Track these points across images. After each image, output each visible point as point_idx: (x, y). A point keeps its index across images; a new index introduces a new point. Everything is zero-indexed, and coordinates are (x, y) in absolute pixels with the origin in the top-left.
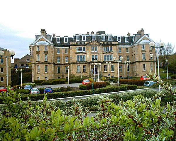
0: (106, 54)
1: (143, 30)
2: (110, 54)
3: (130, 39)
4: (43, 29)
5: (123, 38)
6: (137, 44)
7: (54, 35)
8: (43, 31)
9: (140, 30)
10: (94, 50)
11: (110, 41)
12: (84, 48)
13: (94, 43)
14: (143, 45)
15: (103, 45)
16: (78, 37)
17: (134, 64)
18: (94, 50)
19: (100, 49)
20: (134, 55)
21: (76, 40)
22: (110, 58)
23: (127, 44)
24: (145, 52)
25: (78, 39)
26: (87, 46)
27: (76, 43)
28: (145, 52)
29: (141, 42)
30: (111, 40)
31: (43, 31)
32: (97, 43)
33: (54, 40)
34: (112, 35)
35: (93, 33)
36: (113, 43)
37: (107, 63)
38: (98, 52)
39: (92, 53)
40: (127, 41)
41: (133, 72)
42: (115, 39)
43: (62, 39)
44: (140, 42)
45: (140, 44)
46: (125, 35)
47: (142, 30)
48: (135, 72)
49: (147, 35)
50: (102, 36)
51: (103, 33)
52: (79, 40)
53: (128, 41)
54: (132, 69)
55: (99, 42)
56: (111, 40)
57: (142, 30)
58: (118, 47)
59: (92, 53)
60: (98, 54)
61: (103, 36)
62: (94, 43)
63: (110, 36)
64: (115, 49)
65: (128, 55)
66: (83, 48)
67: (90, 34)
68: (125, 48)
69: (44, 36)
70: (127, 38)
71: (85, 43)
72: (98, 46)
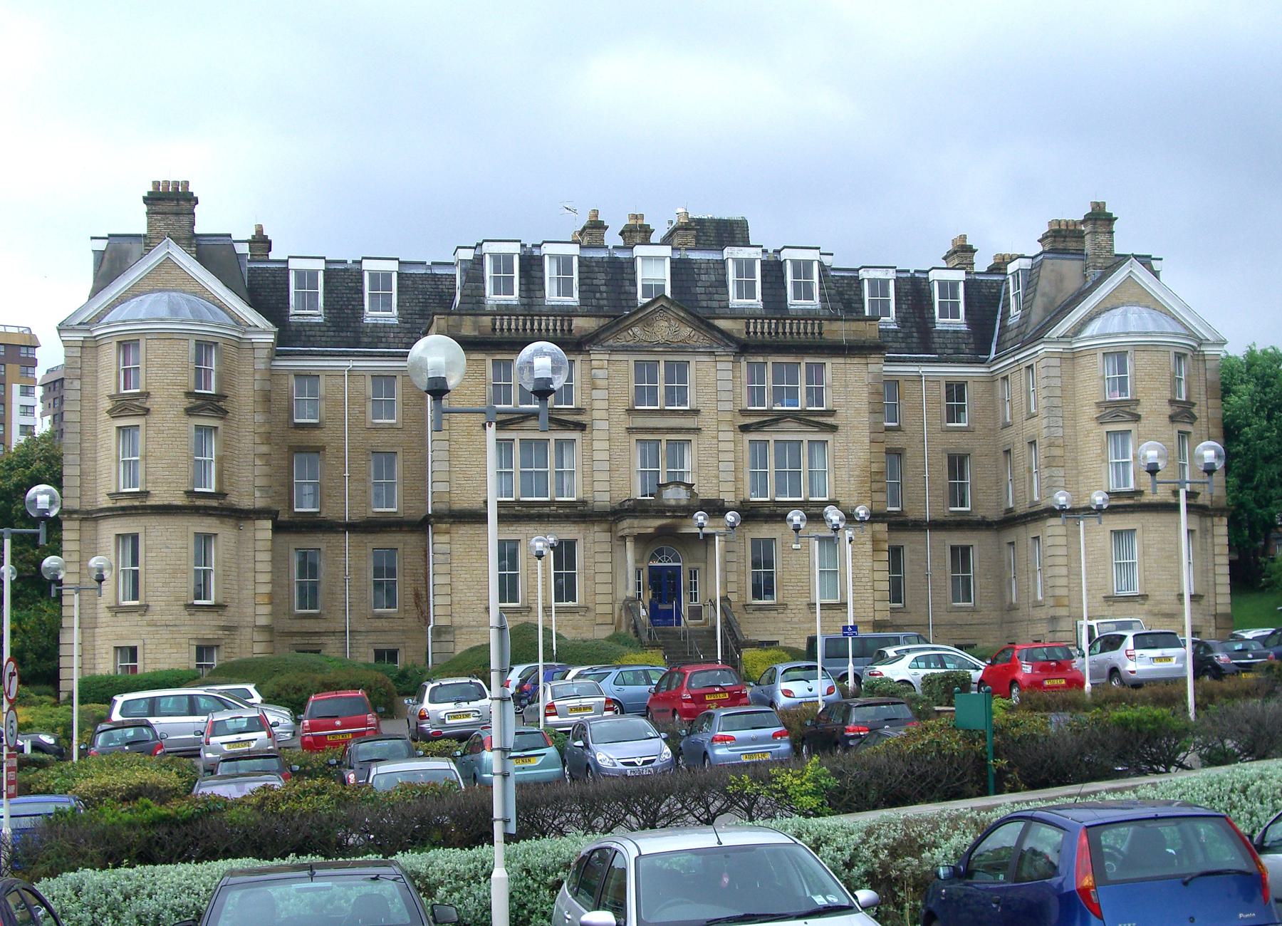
0: (772, 438)
1: (1110, 220)
2: (806, 438)
3: (984, 298)
4: (171, 173)
5: (914, 291)
6: (1058, 348)
7: (261, 242)
8: (171, 203)
9: (1076, 212)
10: (661, 392)
11: (807, 316)
12: (815, 374)
13: (664, 329)
14: (1119, 356)
15: (744, 348)
16: (503, 262)
17: (1022, 535)
18: (661, 392)
19: (716, 383)
20: (1020, 449)
21: (492, 298)
22: (804, 469)
23: (952, 350)
24: (1137, 418)
25: (503, 285)
26: (599, 357)
27: (487, 320)
28: (1137, 418)
29: (1093, 328)
30: (815, 303)
31: (171, 203)
32: (686, 331)
33: (263, 284)
34: (827, 260)
35: (637, 232)
36: (840, 331)
37: (796, 516)
38: (695, 412)
39: (640, 422)
40: (952, 322)
41: (1012, 608)
42: (843, 290)
43: (343, 282)
44: (1088, 332)
45: (1091, 351)
46: (926, 257)
47: (1100, 218)
48: (1038, 605)
49: (1145, 261)
50: (730, 264)
51: (730, 232)
52: (514, 298)
53: (960, 323)
54: (1001, 582)
55: (703, 322)
56: (815, 303)
57: (1100, 218)
58: (878, 367)
59: (640, 422)
60: (697, 430)
61: (745, 267)
62: (664, 329)
63: (802, 268)
64: (847, 385)
65: (959, 443)
66: (802, 370)
67: (612, 238)
68: (933, 380)
69: (177, 240)
70: (948, 288)
71: (578, 323)
72: (693, 360)
